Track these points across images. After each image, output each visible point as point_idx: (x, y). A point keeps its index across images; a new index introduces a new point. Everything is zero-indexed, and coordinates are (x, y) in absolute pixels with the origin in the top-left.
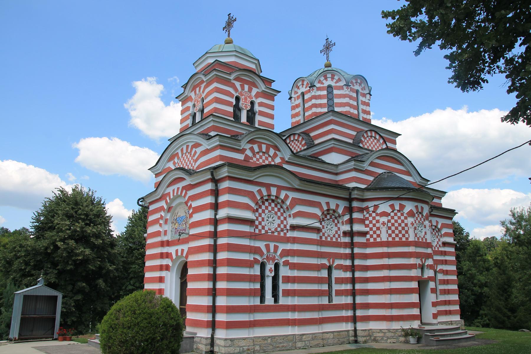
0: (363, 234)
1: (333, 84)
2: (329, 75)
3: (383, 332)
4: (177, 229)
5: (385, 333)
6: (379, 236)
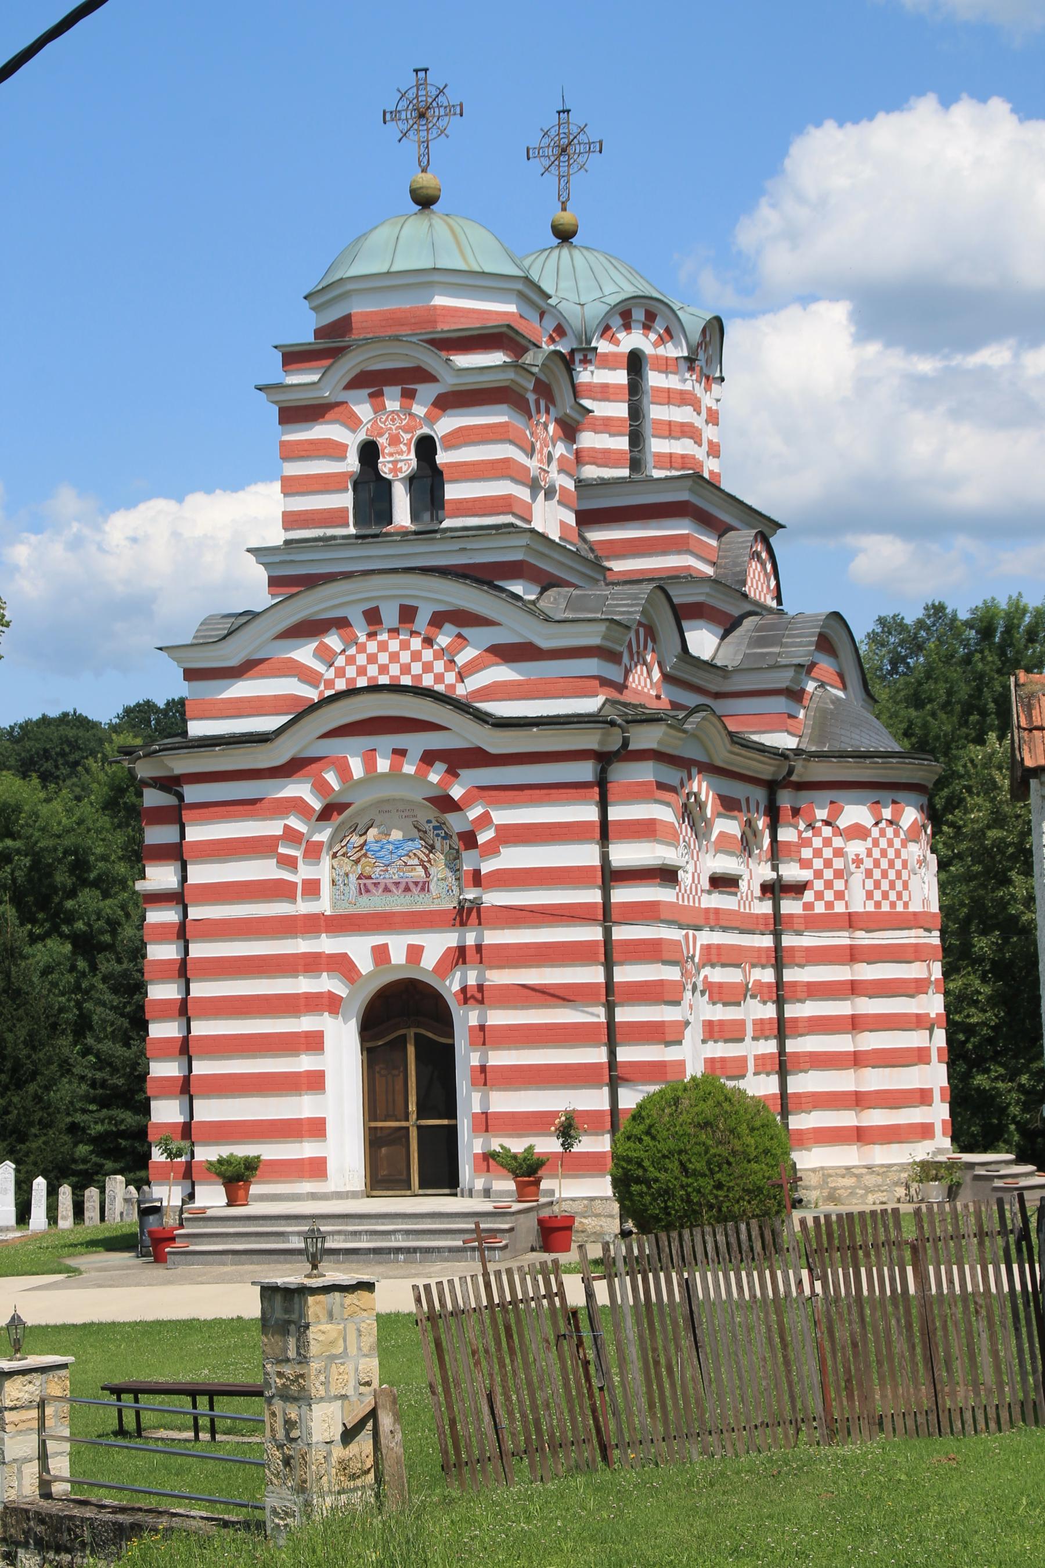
0: (798, 889)
1: (648, 349)
2: (638, 315)
3: (856, 1176)
4: (370, 877)
5: (858, 1176)
6: (839, 895)
